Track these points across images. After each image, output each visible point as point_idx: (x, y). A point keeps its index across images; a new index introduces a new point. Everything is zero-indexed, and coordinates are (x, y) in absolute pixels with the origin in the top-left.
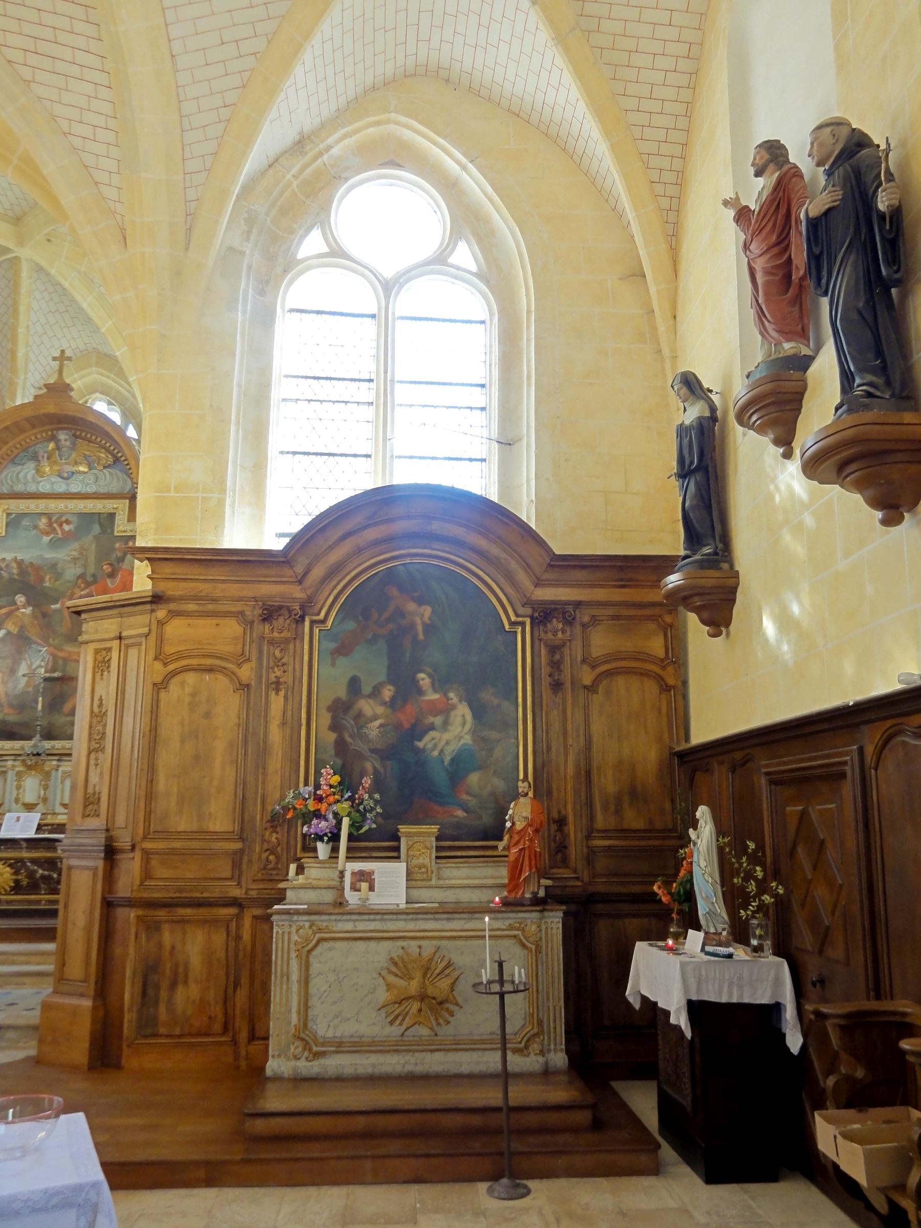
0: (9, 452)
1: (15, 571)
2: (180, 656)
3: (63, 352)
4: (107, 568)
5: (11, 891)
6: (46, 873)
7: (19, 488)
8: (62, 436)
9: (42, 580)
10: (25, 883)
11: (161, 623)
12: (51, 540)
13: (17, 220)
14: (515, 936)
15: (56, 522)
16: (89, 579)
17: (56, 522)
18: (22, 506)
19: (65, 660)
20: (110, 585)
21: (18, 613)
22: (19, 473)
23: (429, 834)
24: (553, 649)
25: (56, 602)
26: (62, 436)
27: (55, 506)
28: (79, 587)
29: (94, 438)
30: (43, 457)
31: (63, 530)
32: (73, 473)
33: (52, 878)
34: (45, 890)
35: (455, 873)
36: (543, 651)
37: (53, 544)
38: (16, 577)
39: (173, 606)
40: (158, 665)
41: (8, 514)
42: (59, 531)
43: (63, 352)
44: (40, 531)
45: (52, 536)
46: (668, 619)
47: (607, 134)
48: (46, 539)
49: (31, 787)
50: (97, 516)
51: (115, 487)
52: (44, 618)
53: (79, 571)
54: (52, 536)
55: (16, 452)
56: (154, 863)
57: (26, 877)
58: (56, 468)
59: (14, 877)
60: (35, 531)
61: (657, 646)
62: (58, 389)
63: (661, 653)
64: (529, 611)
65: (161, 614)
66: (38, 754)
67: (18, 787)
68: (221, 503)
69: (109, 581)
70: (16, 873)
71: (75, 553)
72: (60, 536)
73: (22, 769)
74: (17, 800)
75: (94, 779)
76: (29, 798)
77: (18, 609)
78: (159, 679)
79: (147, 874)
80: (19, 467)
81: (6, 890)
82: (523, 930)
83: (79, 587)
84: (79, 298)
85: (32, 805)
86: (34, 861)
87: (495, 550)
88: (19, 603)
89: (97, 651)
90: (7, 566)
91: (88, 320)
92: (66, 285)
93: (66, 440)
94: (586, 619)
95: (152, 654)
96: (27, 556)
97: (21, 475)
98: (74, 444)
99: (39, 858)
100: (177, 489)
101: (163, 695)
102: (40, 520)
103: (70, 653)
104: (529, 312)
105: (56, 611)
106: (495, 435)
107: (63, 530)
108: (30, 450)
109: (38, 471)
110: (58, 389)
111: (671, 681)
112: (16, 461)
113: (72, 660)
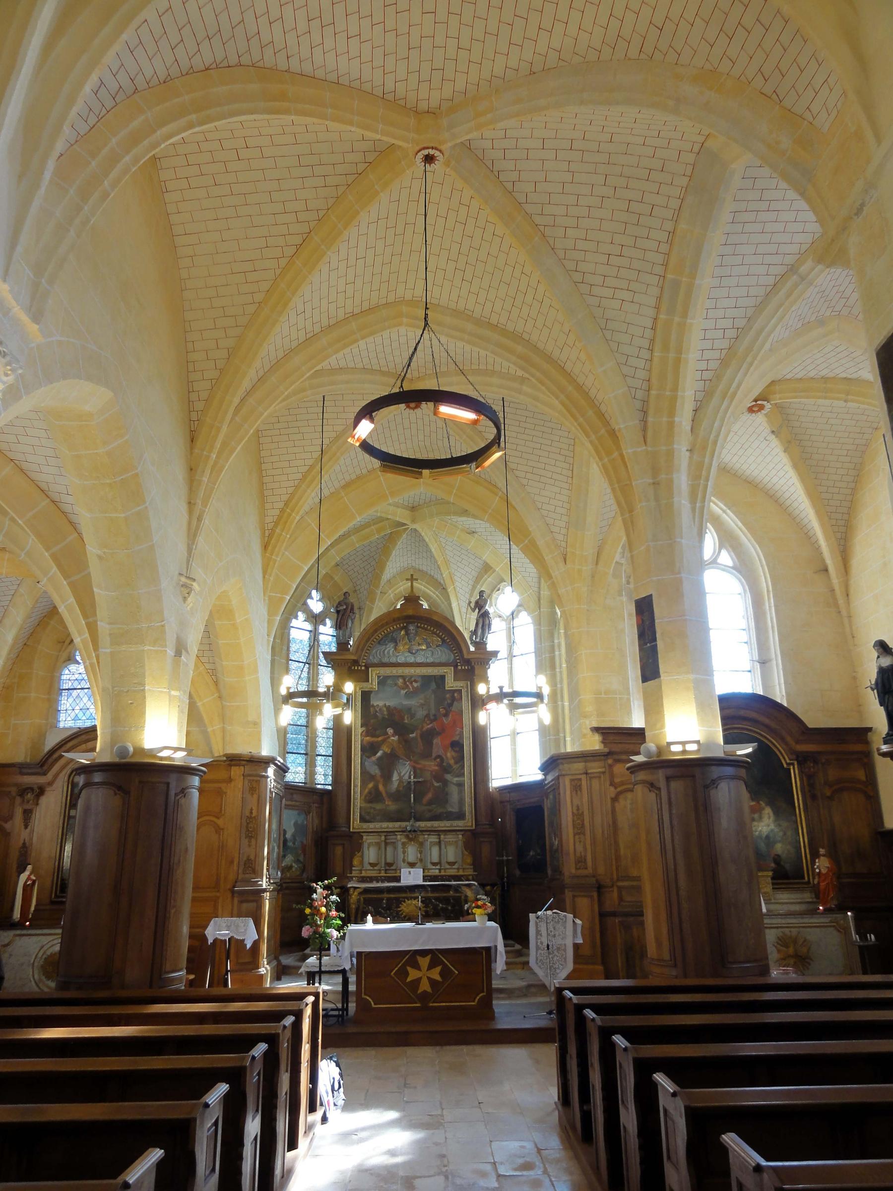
2: (622, 783)
3: (412, 575)
4: (442, 711)
7: (385, 660)
8: (411, 627)
9: (404, 719)
11: (611, 766)
13: (413, 509)
14: (834, 926)
16: (432, 718)
18: (388, 671)
23: (767, 876)
24: (810, 777)
26: (411, 627)
27: (407, 671)
31: (413, 687)
35: (781, 896)
36: (805, 779)
37: (408, 695)
39: (616, 757)
40: (612, 789)
41: (379, 677)
43: (412, 575)
46: (865, 760)
47: (814, 505)
48: (403, 692)
49: (412, 853)
51: (444, 659)
52: (406, 742)
53: (425, 713)
56: (623, 893)
61: (861, 775)
62: (412, 600)
63: (863, 778)
64: (794, 757)
65: (610, 761)
66: (415, 831)
67: (404, 852)
68: (629, 700)
71: (422, 701)
73: (404, 840)
74: (404, 861)
75: (580, 848)
76: (411, 858)
78: (613, 796)
79: (621, 899)
82: (837, 922)
84: (431, 546)
86: (437, 899)
87: (773, 725)
89: (572, 780)
91: (432, 556)
92: (427, 540)
94: (824, 761)
95: (608, 783)
96: (391, 703)
98: (417, 632)
100: (606, 693)
101: (616, 804)
104: (768, 591)
105: (413, 738)
106: (756, 657)
107: (413, 687)
109: (395, 649)
110: (412, 600)
111: (872, 794)
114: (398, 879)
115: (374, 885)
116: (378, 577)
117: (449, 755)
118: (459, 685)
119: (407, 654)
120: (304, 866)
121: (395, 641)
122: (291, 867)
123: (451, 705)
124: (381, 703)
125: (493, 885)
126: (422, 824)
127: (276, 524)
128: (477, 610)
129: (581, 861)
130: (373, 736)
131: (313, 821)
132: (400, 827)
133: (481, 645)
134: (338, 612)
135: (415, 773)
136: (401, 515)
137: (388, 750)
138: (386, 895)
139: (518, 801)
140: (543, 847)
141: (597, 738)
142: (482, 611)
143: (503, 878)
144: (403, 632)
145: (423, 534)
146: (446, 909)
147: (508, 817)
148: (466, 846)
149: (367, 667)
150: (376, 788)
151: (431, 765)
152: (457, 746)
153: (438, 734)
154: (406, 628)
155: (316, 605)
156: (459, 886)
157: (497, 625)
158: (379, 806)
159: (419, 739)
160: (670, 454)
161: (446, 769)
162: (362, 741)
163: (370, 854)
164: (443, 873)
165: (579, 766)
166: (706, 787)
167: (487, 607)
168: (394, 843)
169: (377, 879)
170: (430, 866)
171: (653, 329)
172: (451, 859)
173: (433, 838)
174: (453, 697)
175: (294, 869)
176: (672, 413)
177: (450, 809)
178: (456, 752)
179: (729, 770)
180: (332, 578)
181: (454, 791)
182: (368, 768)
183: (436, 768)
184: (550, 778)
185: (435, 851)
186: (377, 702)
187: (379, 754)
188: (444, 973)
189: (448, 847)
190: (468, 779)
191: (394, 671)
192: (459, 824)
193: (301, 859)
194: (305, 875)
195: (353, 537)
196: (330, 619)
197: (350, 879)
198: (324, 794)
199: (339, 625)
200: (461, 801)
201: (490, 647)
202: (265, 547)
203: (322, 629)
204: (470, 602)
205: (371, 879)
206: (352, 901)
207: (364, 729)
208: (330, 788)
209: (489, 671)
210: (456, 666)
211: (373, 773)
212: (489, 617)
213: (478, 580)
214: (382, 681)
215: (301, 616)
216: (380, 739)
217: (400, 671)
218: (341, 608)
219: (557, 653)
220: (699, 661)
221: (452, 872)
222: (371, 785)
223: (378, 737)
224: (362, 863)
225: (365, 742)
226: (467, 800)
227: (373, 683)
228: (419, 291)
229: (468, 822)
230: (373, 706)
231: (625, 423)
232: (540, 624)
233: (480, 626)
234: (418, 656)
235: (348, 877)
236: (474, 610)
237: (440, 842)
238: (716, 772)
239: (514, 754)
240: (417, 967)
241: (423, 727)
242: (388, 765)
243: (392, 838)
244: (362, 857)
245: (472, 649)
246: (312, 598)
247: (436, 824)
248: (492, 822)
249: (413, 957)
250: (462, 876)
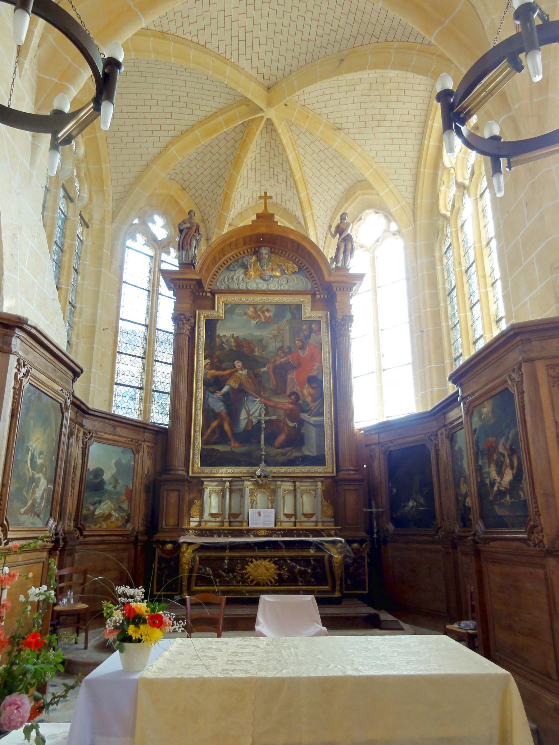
0: (226, 262)
1: (233, 344)
3: (266, 193)
5: (276, 583)
6: (303, 568)
7: (235, 286)
9: (253, 351)
10: (286, 576)
12: (257, 323)
15: (260, 311)
17: (260, 310)
18: (237, 298)
19: (273, 407)
20: (301, 355)
21: (237, 374)
22: (233, 277)
25: (264, 366)
26: (264, 251)
28: (280, 356)
29: (284, 253)
30: (250, 266)
32: (271, 277)
33: (308, 573)
34: (302, 582)
37: (259, 326)
38: (234, 348)
41: (226, 305)
42: (263, 317)
43: (266, 193)
44: (249, 316)
45: (258, 320)
48: (253, 322)
50: (288, 308)
52: (256, 378)
53: (279, 345)
54: (258, 320)
55: (230, 262)
57: (288, 571)
58: (258, 273)
59: (278, 572)
60: (245, 317)
62: (265, 217)
66: (265, 477)
69: (300, 352)
70: (280, 568)
71: (275, 332)
72: (263, 320)
77: (237, 371)
80: (233, 273)
81: (271, 582)
83: (280, 356)
84: (288, 152)
85: (236, 514)
86: (292, 559)
88: (237, 367)
90: (227, 341)
92: (284, 142)
93: (266, 254)
96: (241, 333)
97: (235, 278)
98: (270, 257)
99: (297, 557)
102: (249, 309)
103: (277, 403)
105: (264, 372)
107: (265, 316)
108: (240, 260)
109: (246, 274)
110: (265, 217)
112: (230, 268)
113: (278, 408)
115: (216, 540)
116: (227, 198)
117: (305, 392)
118: (318, 315)
119: (259, 280)
120: (129, 516)
121: (245, 267)
122: (110, 516)
123: (308, 337)
124: (228, 334)
125: (361, 542)
126: (274, 469)
128: (338, 235)
130: (218, 369)
131: (146, 463)
132: (248, 472)
133: (344, 268)
134: (181, 231)
135: (266, 409)
136: (256, 94)
138: (228, 554)
139: (391, 442)
140: (430, 497)
142: (344, 235)
143: (370, 531)
144: (254, 258)
145: (280, 131)
146: (305, 572)
147: (376, 464)
149: (213, 294)
150: (220, 426)
151: (284, 402)
152: (315, 382)
153: (294, 368)
154: (256, 252)
155: (159, 228)
156: (321, 543)
158: (221, 448)
159: (272, 374)
162: (205, 375)
163: (212, 503)
164: (298, 527)
167: (349, 231)
168: (241, 490)
170: (283, 518)
172: (307, 509)
173: (288, 486)
174: (310, 327)
175: (113, 519)
177: (307, 453)
178: (313, 388)
180: (177, 203)
181: (311, 434)
182: (211, 405)
183: (291, 406)
185: (289, 499)
186: (224, 332)
187: (226, 389)
189: (304, 497)
191: (244, 298)
193: (125, 506)
194: (129, 526)
195: (197, 131)
196: (173, 247)
197: (184, 531)
198: (160, 433)
199: (182, 247)
200: (321, 445)
203: (164, 257)
204: (330, 227)
206: (184, 560)
207: (208, 361)
209: (351, 302)
210: (314, 295)
211: (217, 411)
212: (352, 242)
213: (339, 206)
214: (230, 309)
215: (141, 239)
216: (226, 372)
217: (251, 298)
218: (185, 226)
219: (439, 267)
221: (309, 526)
222: (214, 424)
223: (224, 370)
225: (209, 377)
227: (220, 311)
229: (328, 469)
230: (219, 336)
232: (415, 240)
233: (342, 250)
235: (184, 530)
236: (334, 236)
237: (295, 490)
239: (385, 384)
241: (275, 361)
242: (234, 402)
244: (202, 506)
246: (154, 222)
248: (358, 469)
250: (323, 530)
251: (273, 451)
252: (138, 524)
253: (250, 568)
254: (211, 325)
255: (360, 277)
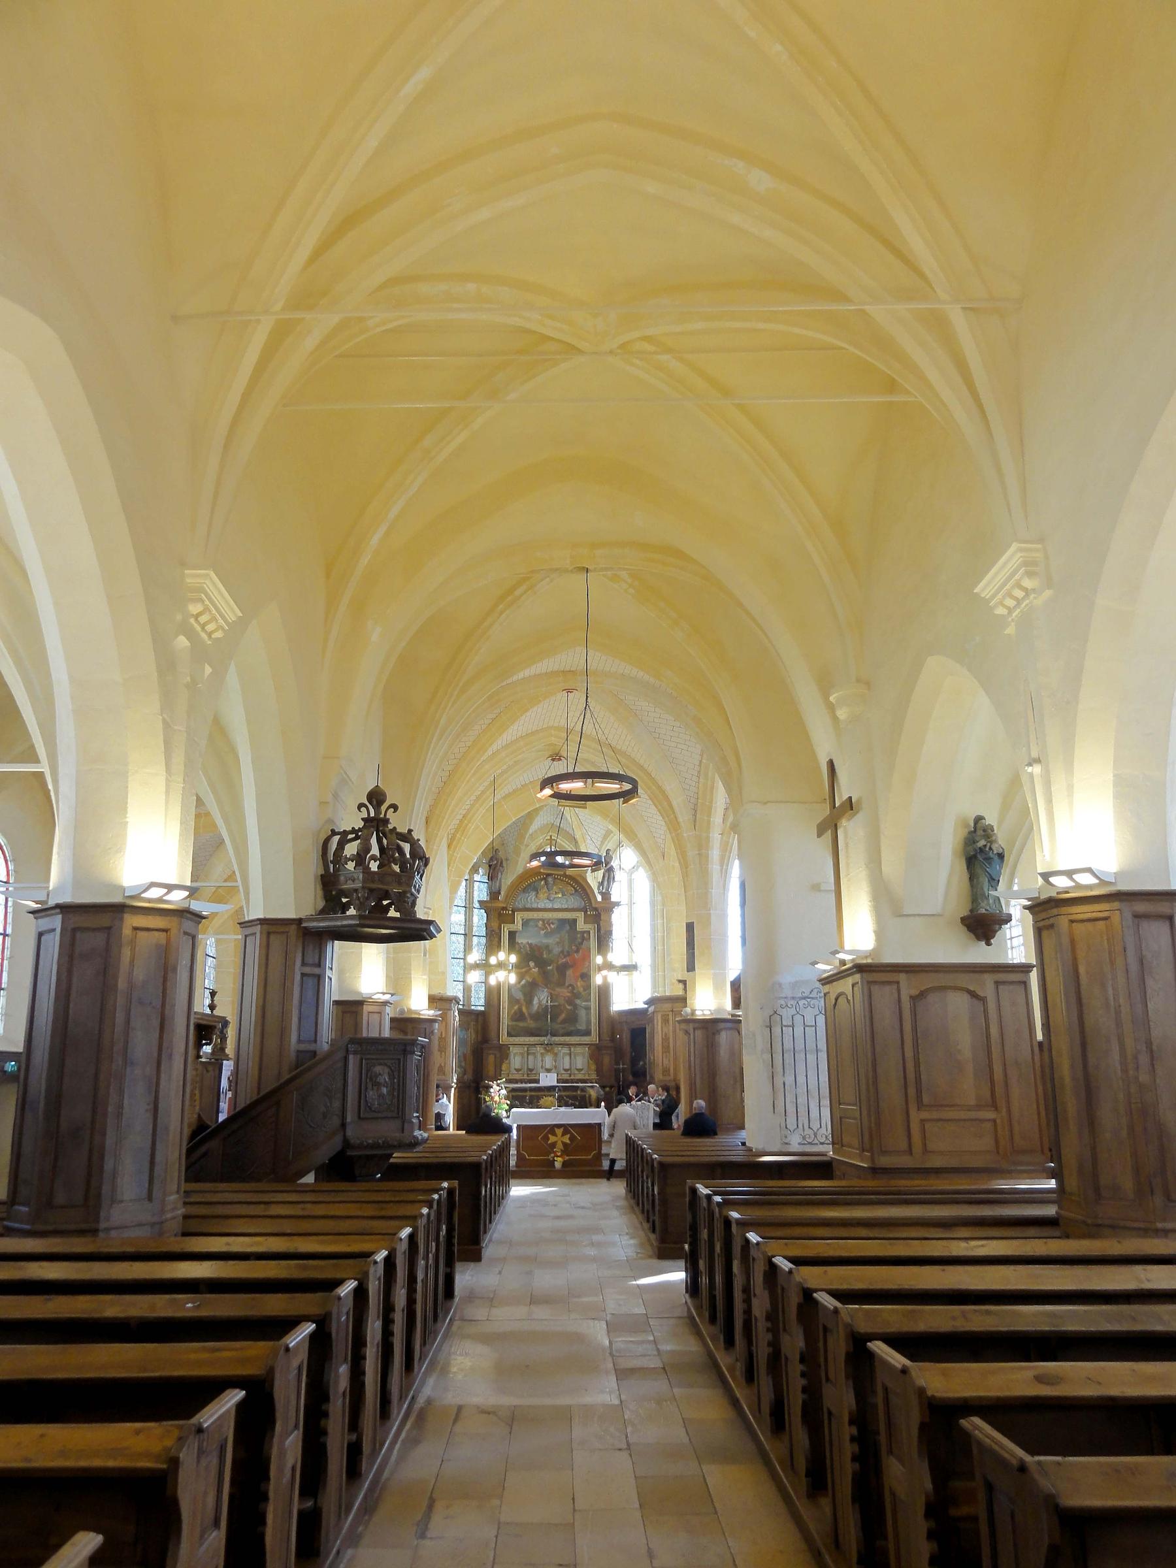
7: (528, 906)
8: (550, 879)
26: (550, 879)
37: (546, 935)
49: (549, 1061)
51: (576, 905)
52: (545, 974)
75: (666, 1062)
96: (532, 941)
114: (537, 1081)
125: (611, 1087)
126: (556, 1039)
127: (457, 830)
129: (666, 1071)
131: (471, 1036)
133: (606, 895)
137: (530, 980)
138: (528, 1093)
141: (681, 986)
148: (592, 1057)
150: (520, 1010)
151: (565, 992)
157: (619, 875)
158: (521, 1024)
160: (708, 838)
161: (577, 996)
165: (667, 1006)
166: (714, 1034)
169: (522, 1081)
171: (700, 765)
173: (566, 1050)
176: (709, 815)
179: (729, 1025)
181: (582, 1013)
184: (651, 1009)
185: (567, 1059)
186: (521, 940)
188: (572, 1138)
190: (593, 1004)
191: (535, 915)
192: (586, 1040)
199: (492, 877)
200: (589, 1022)
201: (614, 899)
202: (449, 846)
203: (477, 877)
205: (516, 1081)
208: (483, 1009)
210: (586, 912)
214: (526, 923)
217: (541, 915)
220: (720, 962)
221: (580, 1076)
224: (509, 1068)
226: (593, 1020)
227: (518, 925)
228: (563, 722)
229: (594, 1038)
231: (684, 817)
234: (554, 903)
238: (722, 1025)
240: (555, 1134)
243: (532, 1050)
245: (599, 898)
247: (567, 1039)
248: (613, 1039)
249: (552, 1129)
251: (556, 1026)
252: (469, 1077)
253: (542, 1102)
254: (512, 935)
255: (618, 904)
